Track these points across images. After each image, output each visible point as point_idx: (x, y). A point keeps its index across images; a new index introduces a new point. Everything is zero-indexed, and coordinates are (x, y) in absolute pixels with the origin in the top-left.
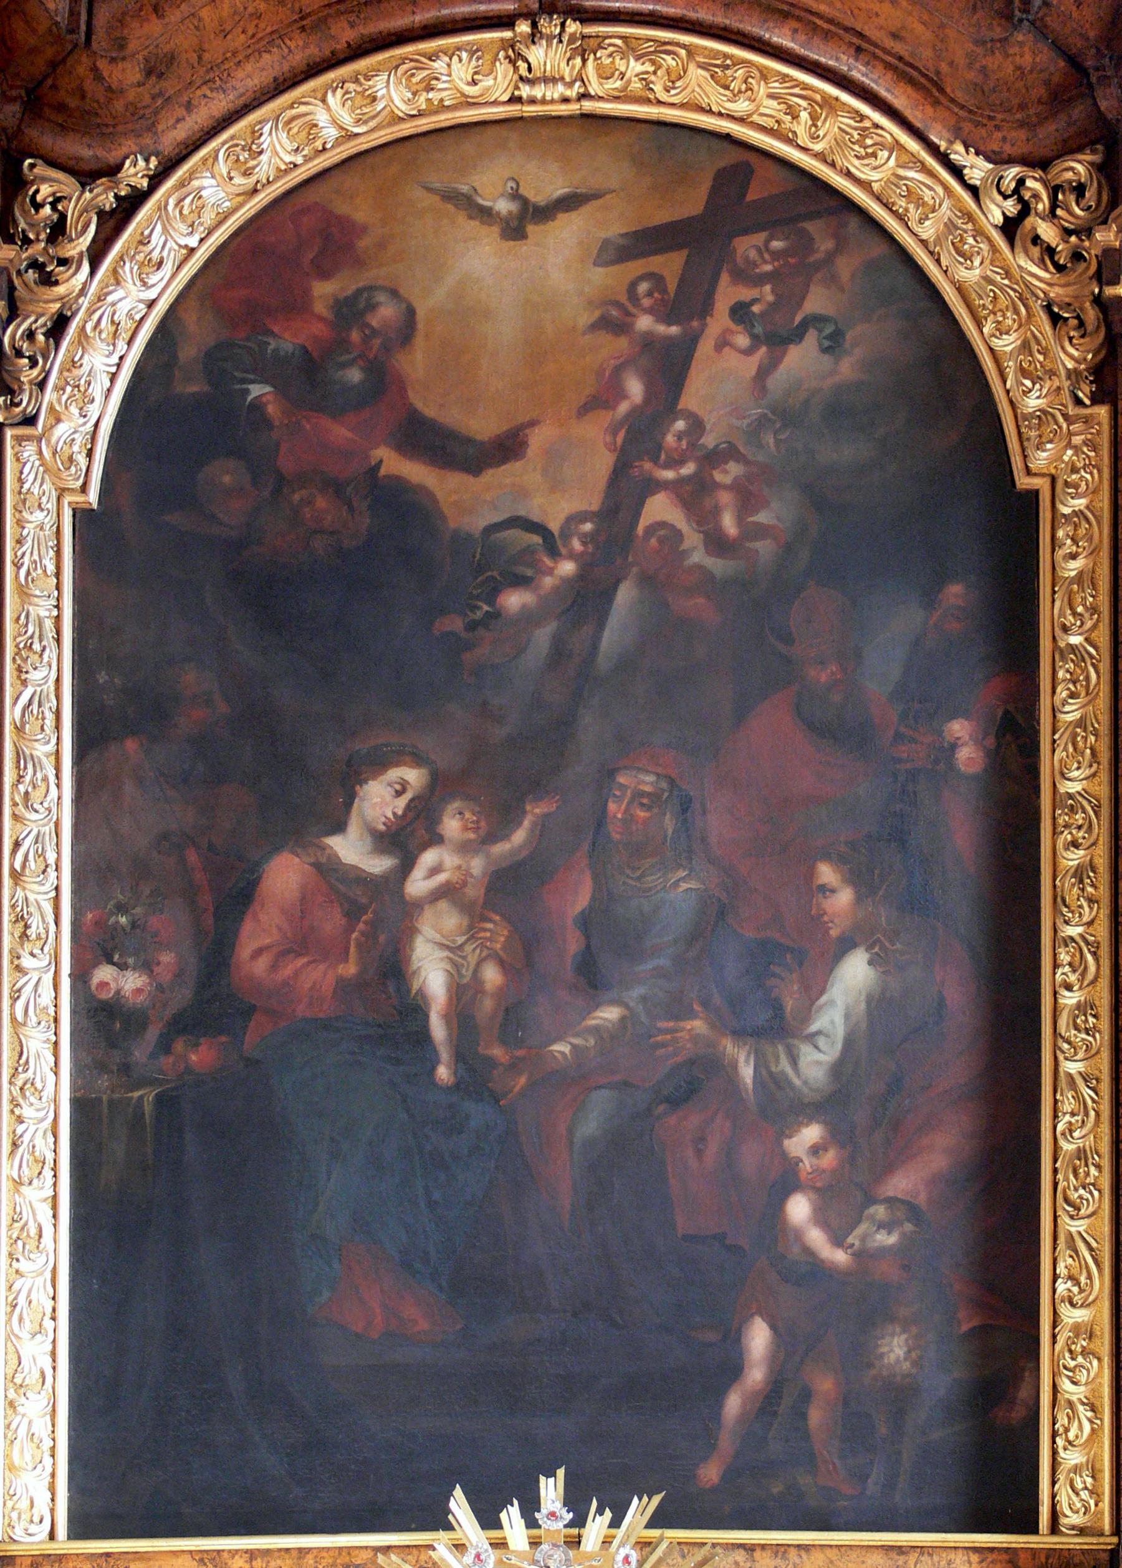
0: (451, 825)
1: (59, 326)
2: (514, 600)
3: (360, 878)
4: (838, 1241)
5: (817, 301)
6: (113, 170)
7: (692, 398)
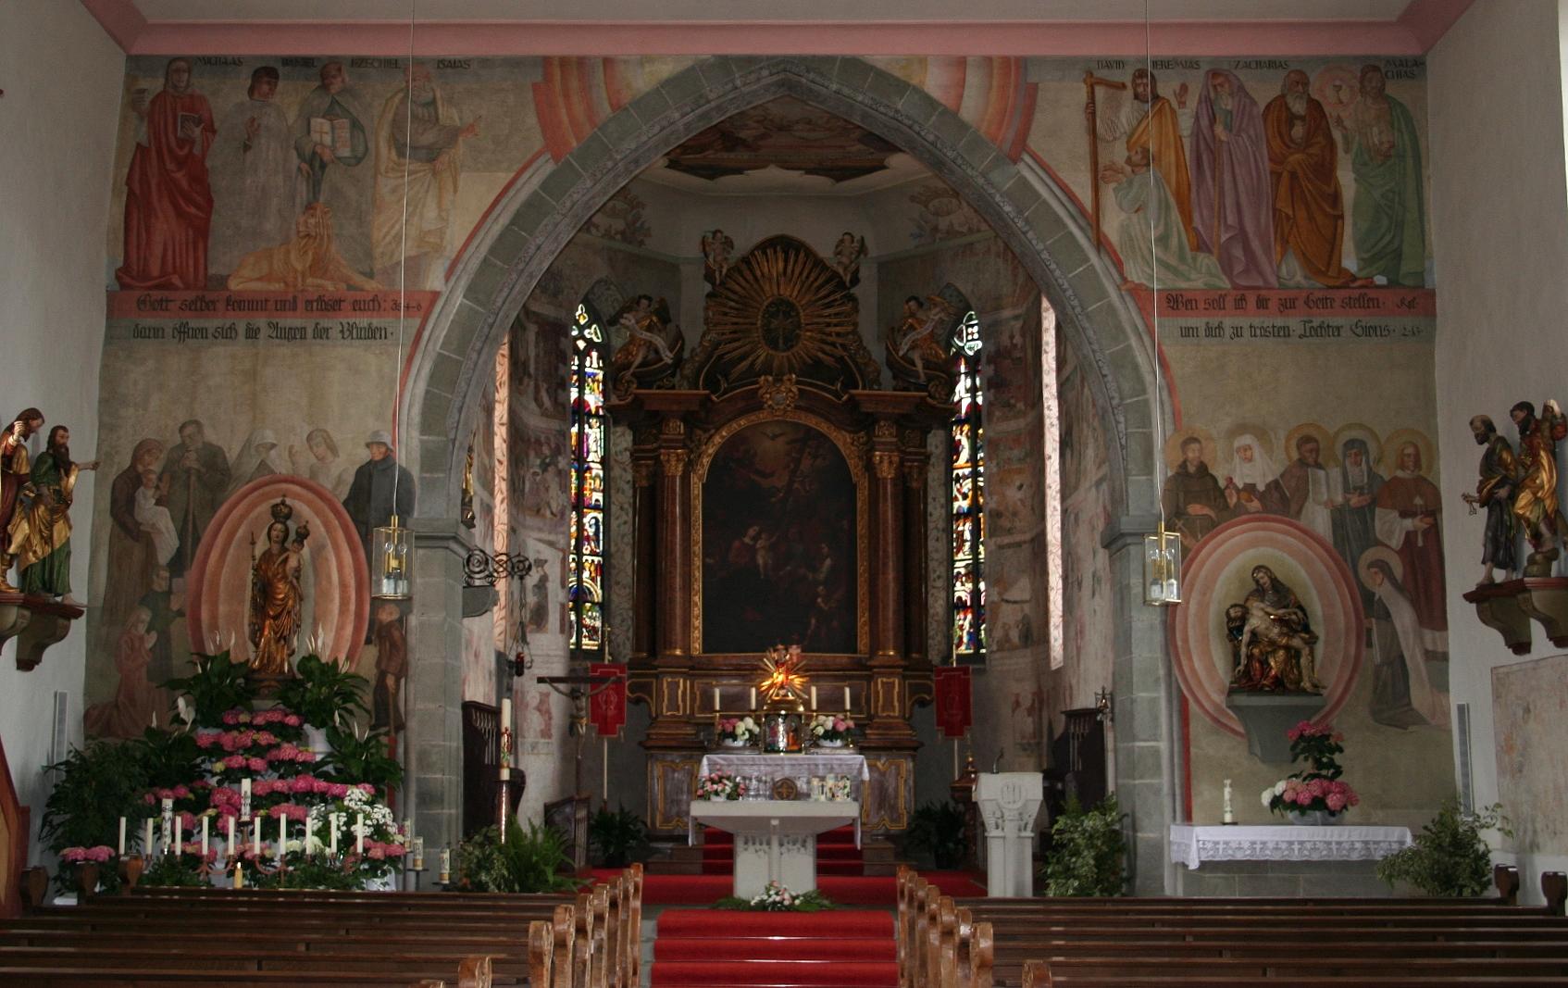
0: (763, 536)
1: (699, 456)
2: (773, 500)
3: (748, 544)
4: (826, 605)
6: (709, 430)
7: (802, 467)
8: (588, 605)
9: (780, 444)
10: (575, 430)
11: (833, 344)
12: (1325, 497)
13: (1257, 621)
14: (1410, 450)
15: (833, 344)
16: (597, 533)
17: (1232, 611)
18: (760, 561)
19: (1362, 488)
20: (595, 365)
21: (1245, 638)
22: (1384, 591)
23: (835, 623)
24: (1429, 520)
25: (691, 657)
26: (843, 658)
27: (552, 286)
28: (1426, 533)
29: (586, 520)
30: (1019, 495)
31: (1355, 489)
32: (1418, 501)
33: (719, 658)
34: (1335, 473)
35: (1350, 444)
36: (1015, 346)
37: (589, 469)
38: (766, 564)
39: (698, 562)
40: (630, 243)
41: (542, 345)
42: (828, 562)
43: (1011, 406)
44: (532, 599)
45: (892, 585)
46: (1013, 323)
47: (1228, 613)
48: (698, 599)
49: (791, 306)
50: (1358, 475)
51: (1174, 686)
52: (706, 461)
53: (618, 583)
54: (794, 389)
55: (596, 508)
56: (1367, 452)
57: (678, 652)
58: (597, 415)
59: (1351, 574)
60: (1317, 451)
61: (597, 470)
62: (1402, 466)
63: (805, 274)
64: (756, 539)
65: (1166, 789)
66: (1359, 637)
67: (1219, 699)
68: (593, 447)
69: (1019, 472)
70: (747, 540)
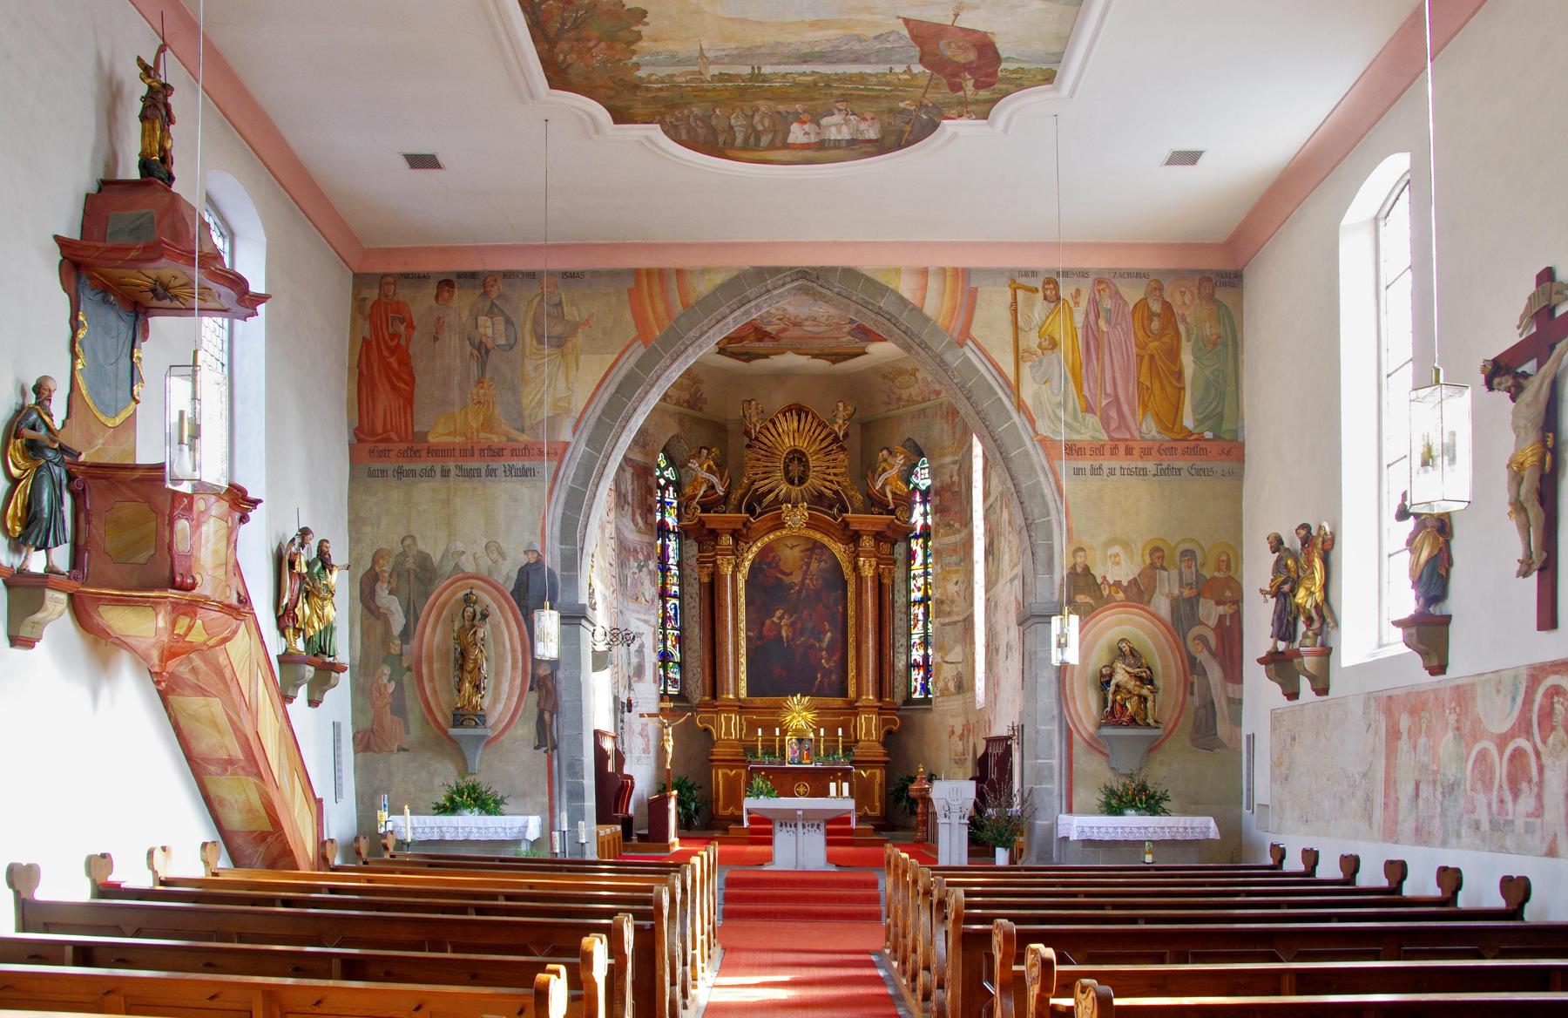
5: (824, 558)
8: (671, 664)
9: (797, 553)
10: (659, 542)
11: (831, 481)
12: (1167, 590)
13: (1121, 676)
14: (1224, 558)
15: (831, 481)
16: (675, 614)
17: (1104, 670)
18: (784, 634)
19: (1191, 584)
20: (672, 496)
21: (1112, 688)
22: (1203, 656)
23: (834, 677)
24: (1235, 607)
25: (739, 700)
26: (838, 702)
28: (1232, 616)
29: (668, 606)
30: (956, 588)
31: (1188, 584)
32: (1228, 594)
33: (758, 701)
34: (1174, 573)
35: (1185, 553)
36: (953, 483)
37: (669, 569)
38: (787, 636)
39: (743, 635)
40: (693, 409)
42: (829, 634)
43: (950, 526)
44: (634, 660)
45: (871, 650)
47: (1101, 671)
48: (743, 660)
49: (803, 454)
50: (1189, 575)
51: (1064, 723)
52: (747, 564)
53: (690, 649)
54: (806, 514)
55: (675, 596)
56: (1195, 558)
57: (731, 696)
58: (674, 532)
59: (1182, 645)
60: (1163, 557)
61: (674, 570)
62: (1218, 569)
64: (781, 618)
65: (1056, 791)
66: (1185, 689)
67: (1091, 729)
68: (671, 554)
69: (957, 572)
70: (775, 619)
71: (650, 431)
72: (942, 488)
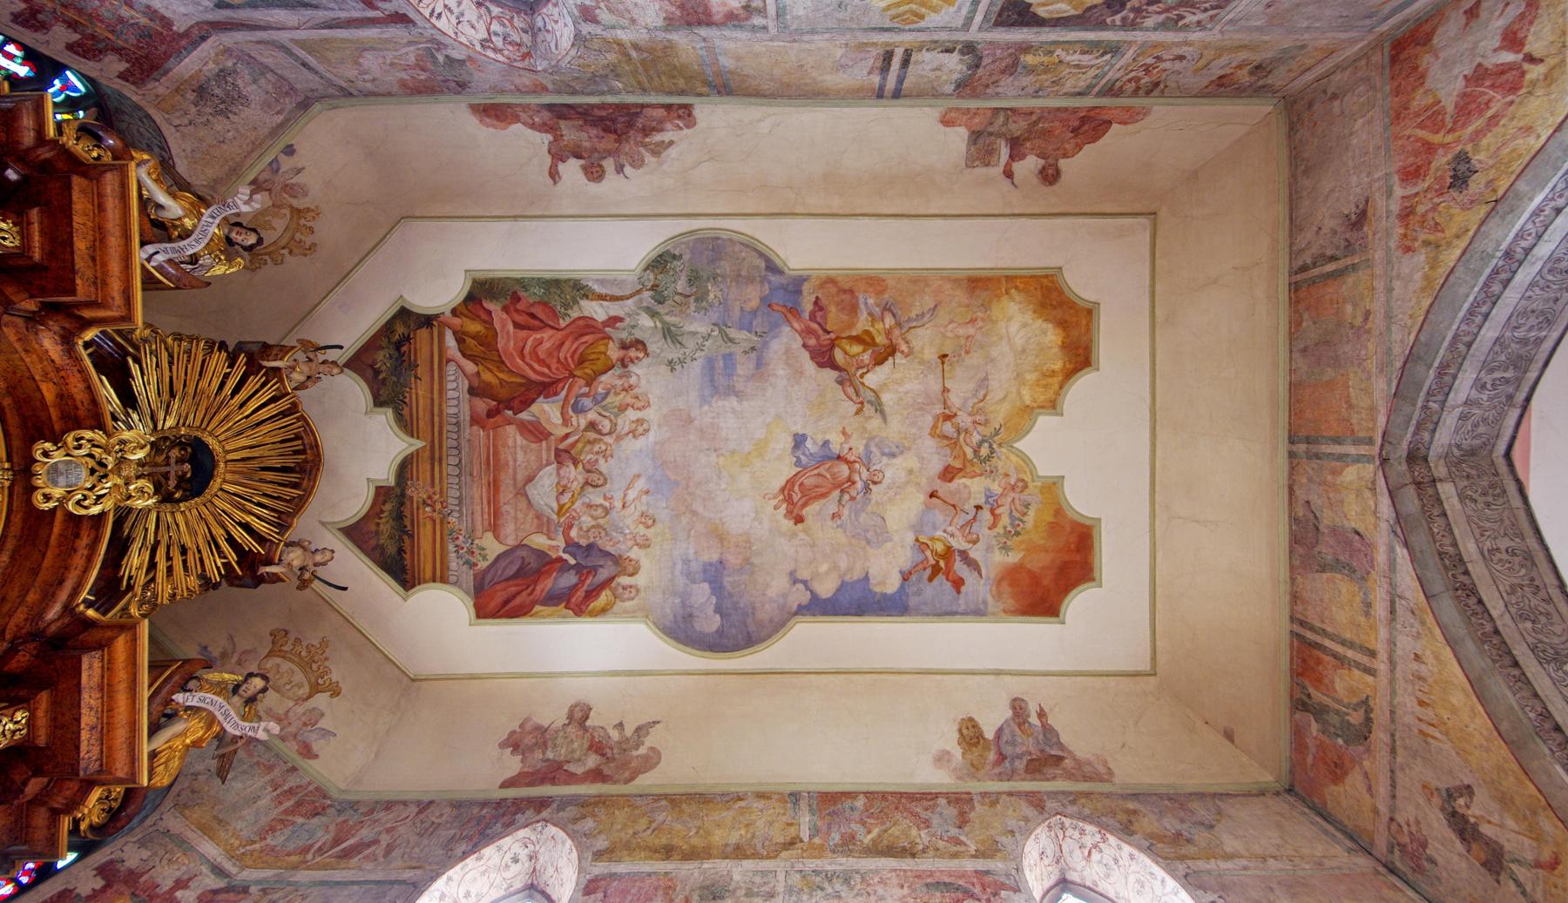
27: (217, 91)
41: (143, 21)
46: (205, 869)
63: (263, 500)
71: (220, 124)
72: (132, 877)
